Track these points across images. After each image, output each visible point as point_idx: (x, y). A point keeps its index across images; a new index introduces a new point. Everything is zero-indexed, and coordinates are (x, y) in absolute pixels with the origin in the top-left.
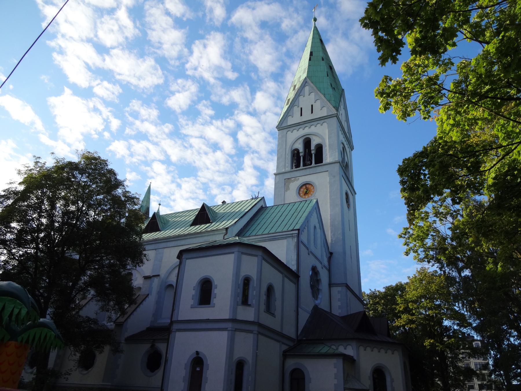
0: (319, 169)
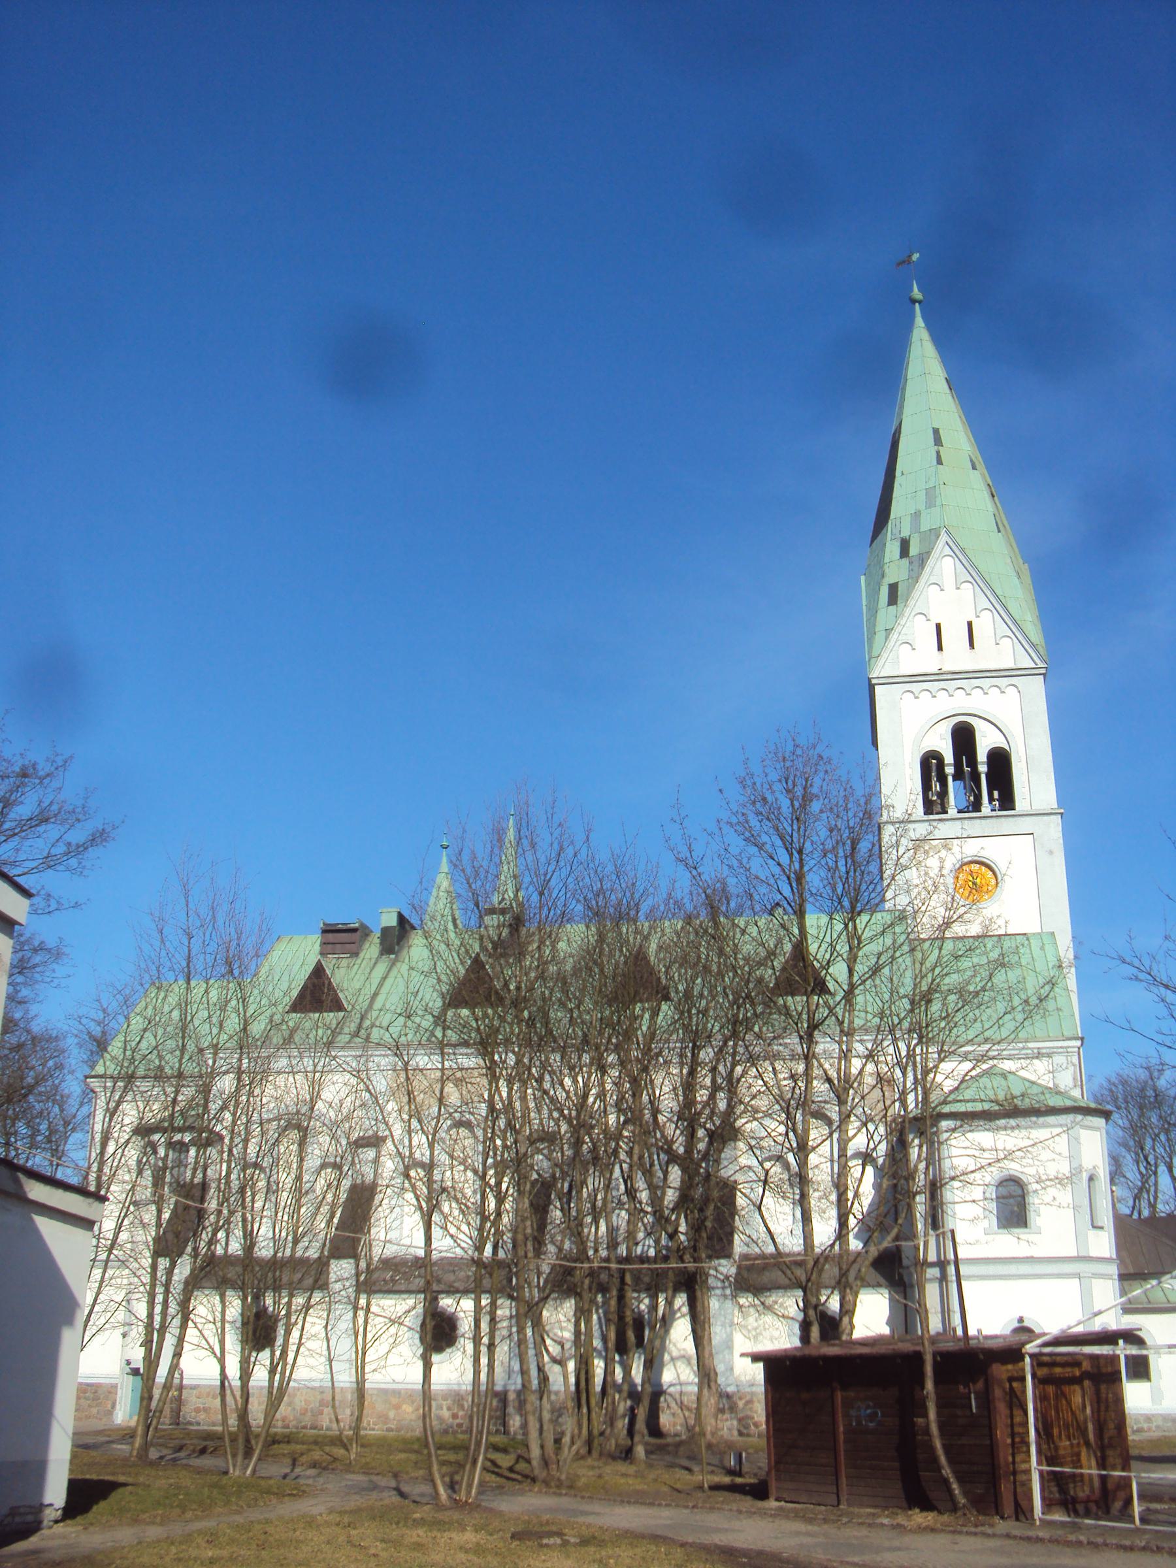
0: (1007, 824)
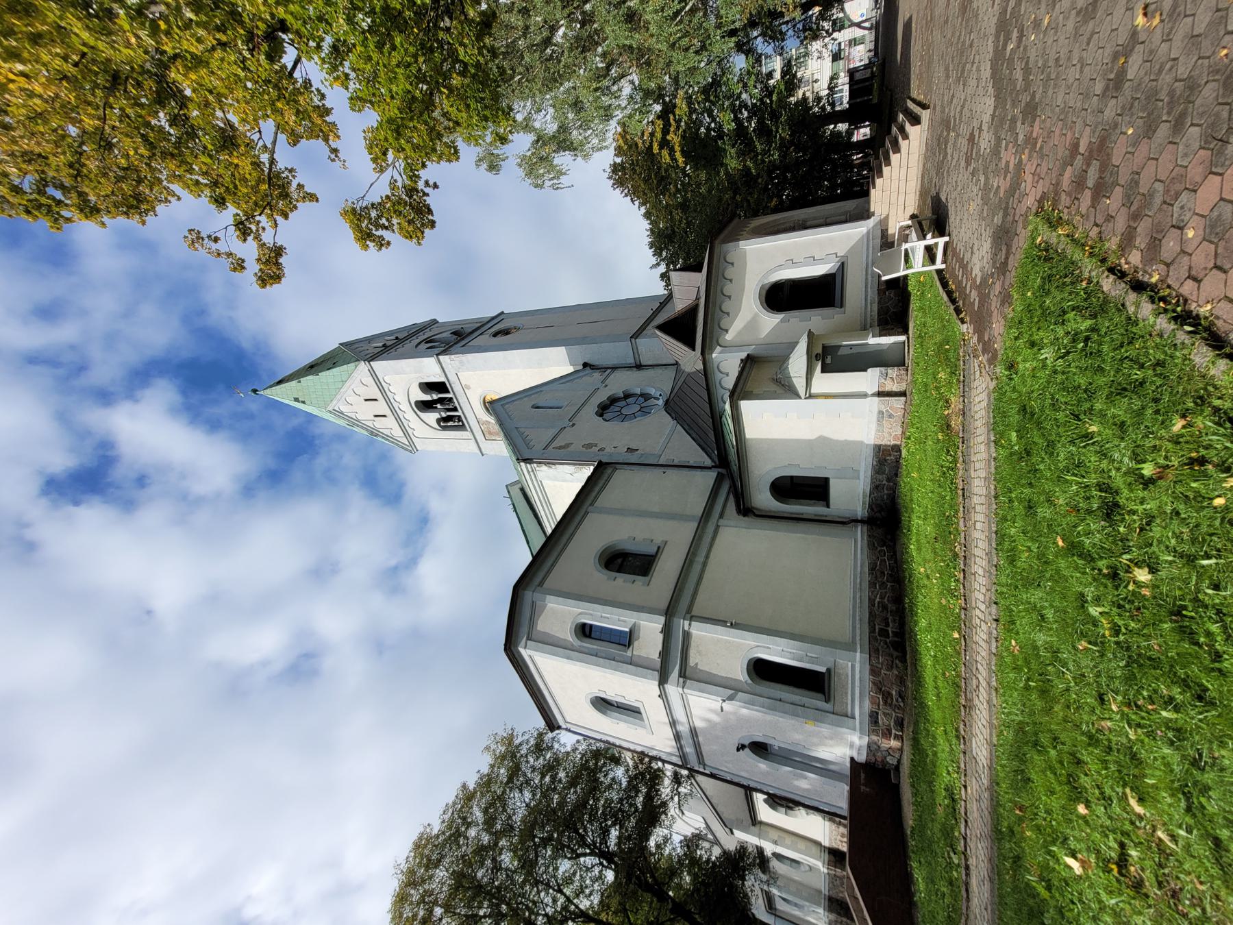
0: (457, 388)
